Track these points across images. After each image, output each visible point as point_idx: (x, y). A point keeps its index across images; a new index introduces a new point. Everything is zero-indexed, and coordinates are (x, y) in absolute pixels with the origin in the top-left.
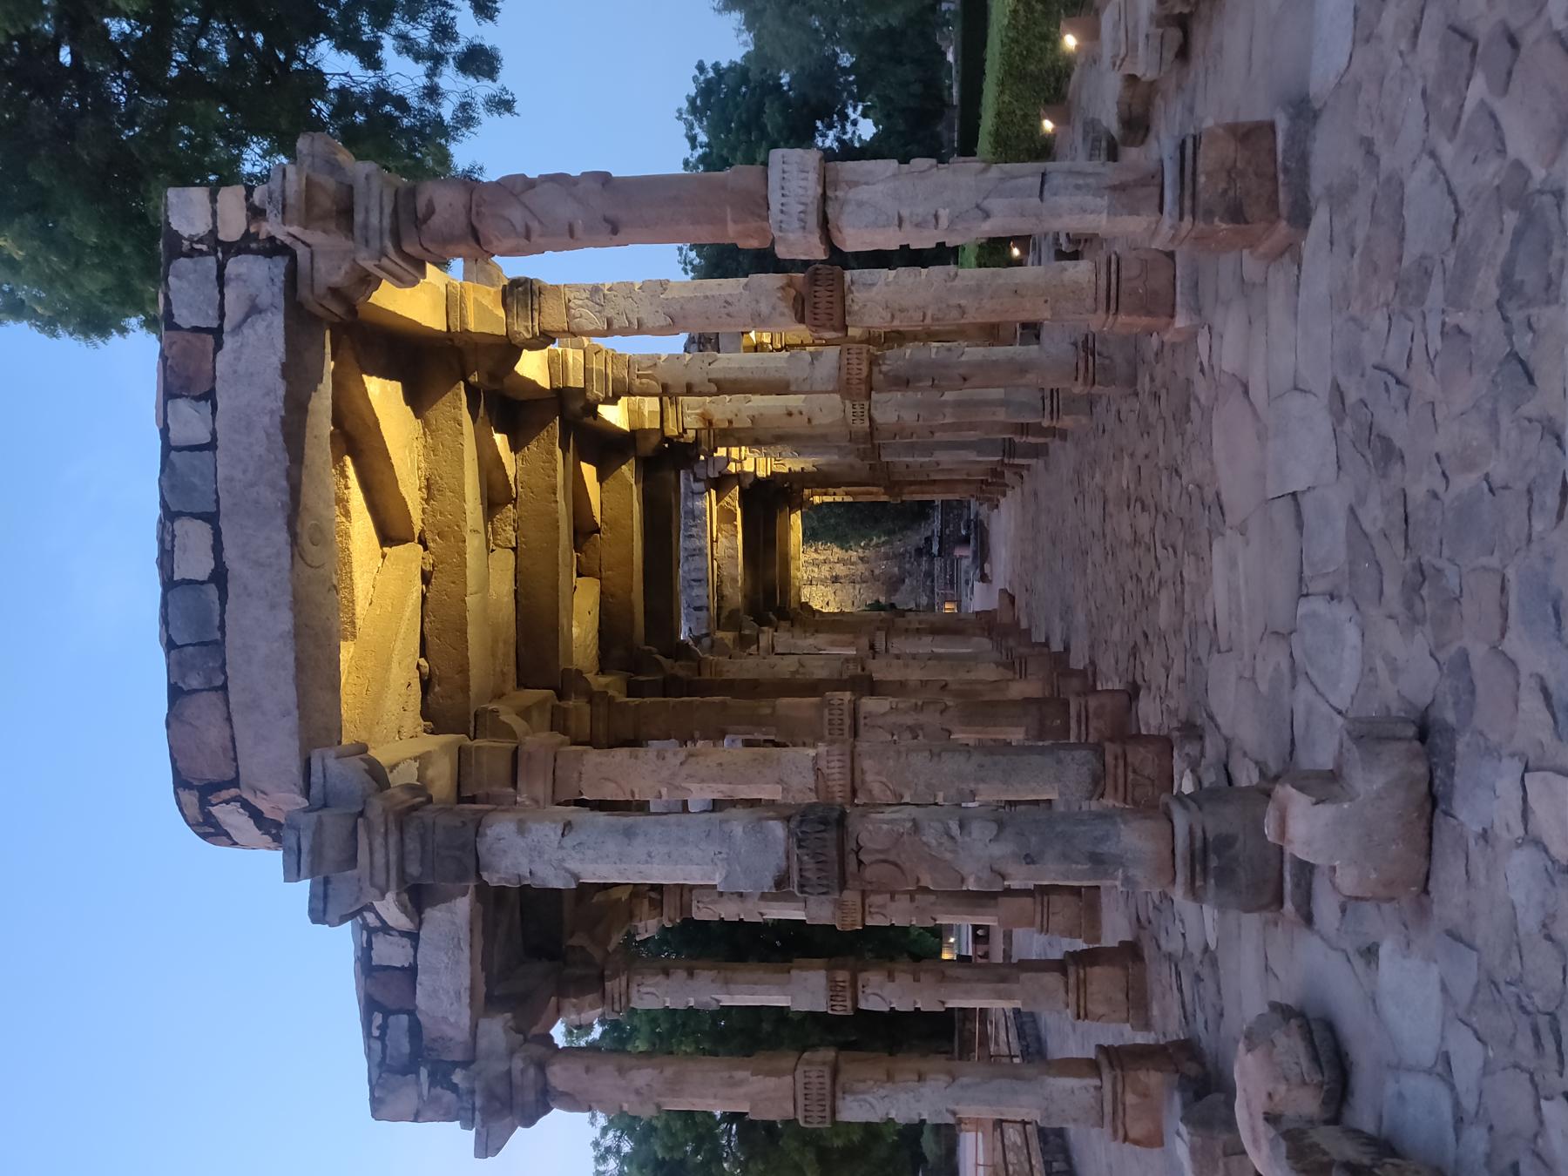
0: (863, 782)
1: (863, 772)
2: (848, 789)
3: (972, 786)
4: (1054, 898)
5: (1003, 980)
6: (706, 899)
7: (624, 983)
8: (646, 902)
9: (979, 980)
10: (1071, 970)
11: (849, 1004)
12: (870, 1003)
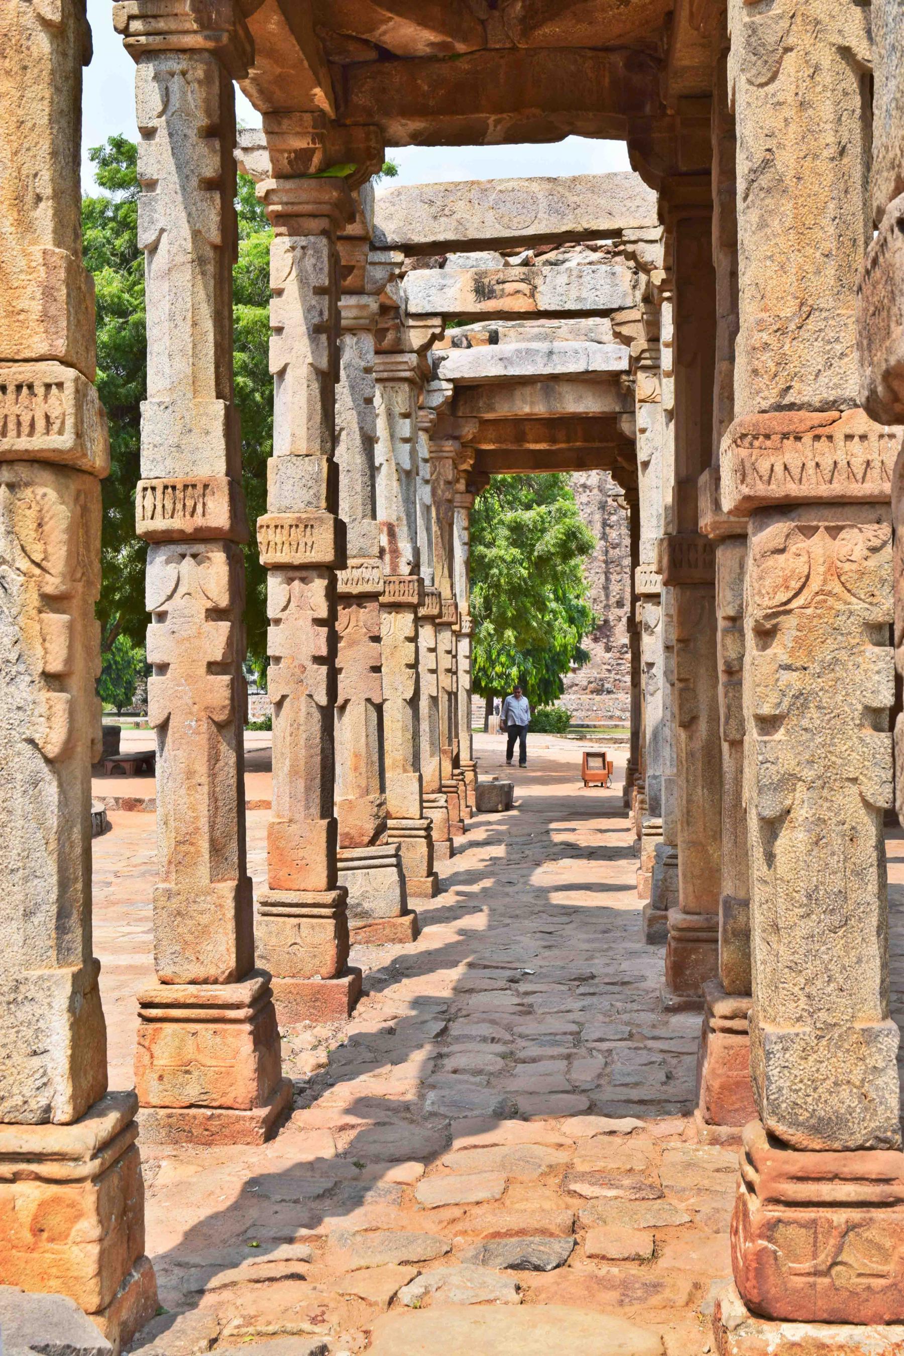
0: (809, 531)
1: (834, 532)
2: (794, 490)
3: (801, 813)
4: (330, 925)
5: (216, 849)
6: (309, 262)
7: (190, 41)
8: (301, 143)
9: (213, 797)
10: (244, 991)
11: (160, 524)
12: (159, 575)
